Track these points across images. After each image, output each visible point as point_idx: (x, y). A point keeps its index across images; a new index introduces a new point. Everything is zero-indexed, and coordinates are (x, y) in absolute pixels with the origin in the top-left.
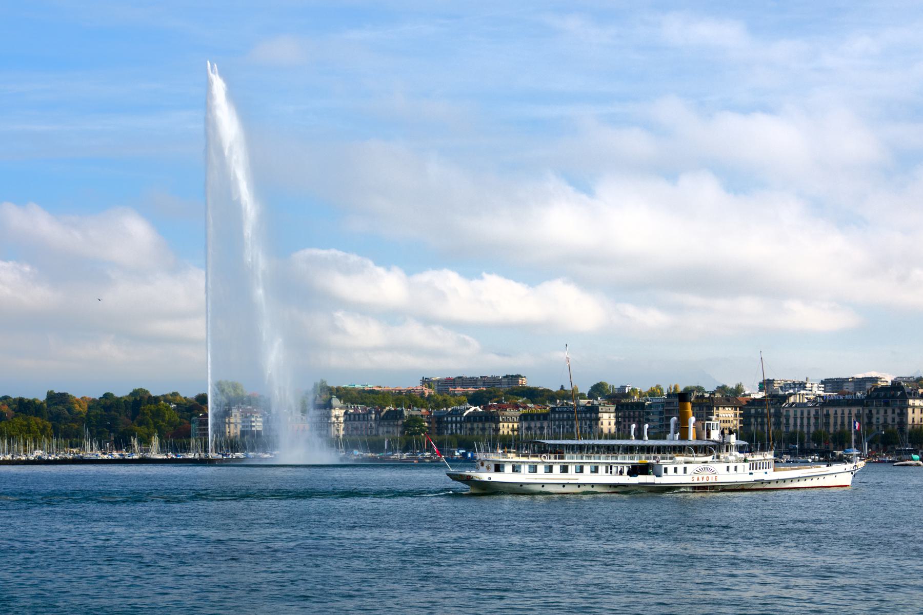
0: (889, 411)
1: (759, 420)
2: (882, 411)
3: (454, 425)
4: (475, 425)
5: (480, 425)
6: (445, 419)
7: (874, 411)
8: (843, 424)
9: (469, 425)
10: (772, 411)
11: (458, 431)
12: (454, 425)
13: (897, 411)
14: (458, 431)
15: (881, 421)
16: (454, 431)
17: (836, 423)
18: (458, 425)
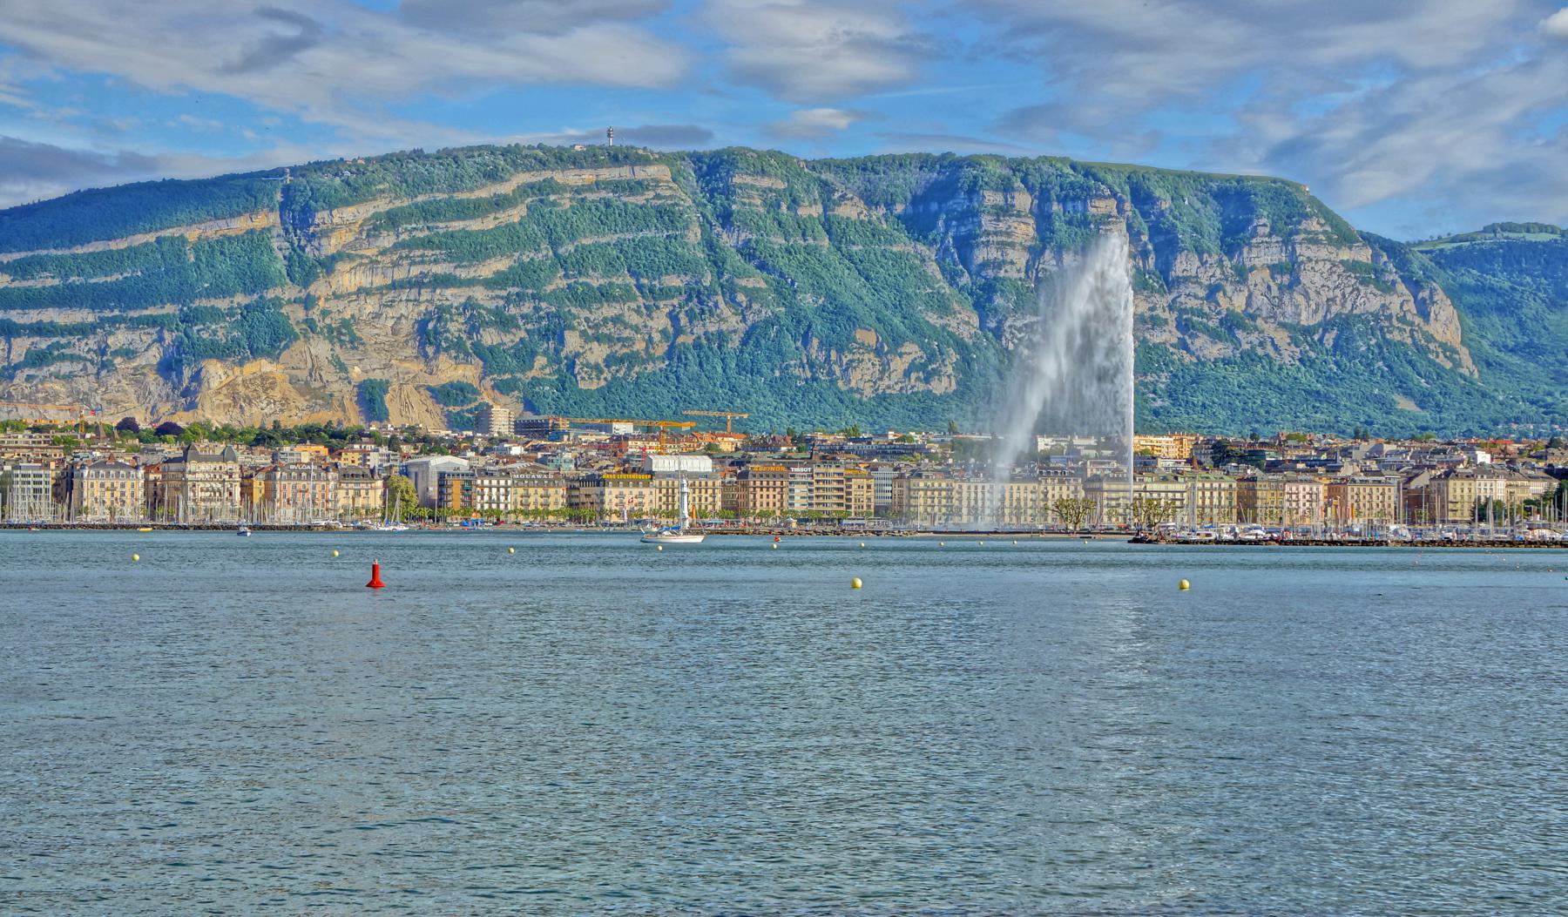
0: (1064, 488)
1: (929, 493)
2: (1057, 488)
3: (494, 490)
4: (531, 491)
5: (541, 491)
6: (479, 482)
7: (1049, 488)
8: (1018, 499)
9: (521, 491)
10: (944, 485)
11: (502, 498)
12: (494, 490)
13: (1072, 488)
14: (502, 498)
15: (1057, 497)
16: (494, 497)
17: (1011, 496)
18: (502, 490)
